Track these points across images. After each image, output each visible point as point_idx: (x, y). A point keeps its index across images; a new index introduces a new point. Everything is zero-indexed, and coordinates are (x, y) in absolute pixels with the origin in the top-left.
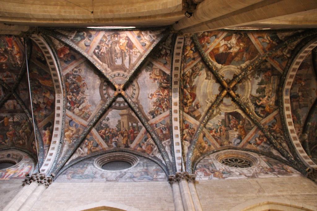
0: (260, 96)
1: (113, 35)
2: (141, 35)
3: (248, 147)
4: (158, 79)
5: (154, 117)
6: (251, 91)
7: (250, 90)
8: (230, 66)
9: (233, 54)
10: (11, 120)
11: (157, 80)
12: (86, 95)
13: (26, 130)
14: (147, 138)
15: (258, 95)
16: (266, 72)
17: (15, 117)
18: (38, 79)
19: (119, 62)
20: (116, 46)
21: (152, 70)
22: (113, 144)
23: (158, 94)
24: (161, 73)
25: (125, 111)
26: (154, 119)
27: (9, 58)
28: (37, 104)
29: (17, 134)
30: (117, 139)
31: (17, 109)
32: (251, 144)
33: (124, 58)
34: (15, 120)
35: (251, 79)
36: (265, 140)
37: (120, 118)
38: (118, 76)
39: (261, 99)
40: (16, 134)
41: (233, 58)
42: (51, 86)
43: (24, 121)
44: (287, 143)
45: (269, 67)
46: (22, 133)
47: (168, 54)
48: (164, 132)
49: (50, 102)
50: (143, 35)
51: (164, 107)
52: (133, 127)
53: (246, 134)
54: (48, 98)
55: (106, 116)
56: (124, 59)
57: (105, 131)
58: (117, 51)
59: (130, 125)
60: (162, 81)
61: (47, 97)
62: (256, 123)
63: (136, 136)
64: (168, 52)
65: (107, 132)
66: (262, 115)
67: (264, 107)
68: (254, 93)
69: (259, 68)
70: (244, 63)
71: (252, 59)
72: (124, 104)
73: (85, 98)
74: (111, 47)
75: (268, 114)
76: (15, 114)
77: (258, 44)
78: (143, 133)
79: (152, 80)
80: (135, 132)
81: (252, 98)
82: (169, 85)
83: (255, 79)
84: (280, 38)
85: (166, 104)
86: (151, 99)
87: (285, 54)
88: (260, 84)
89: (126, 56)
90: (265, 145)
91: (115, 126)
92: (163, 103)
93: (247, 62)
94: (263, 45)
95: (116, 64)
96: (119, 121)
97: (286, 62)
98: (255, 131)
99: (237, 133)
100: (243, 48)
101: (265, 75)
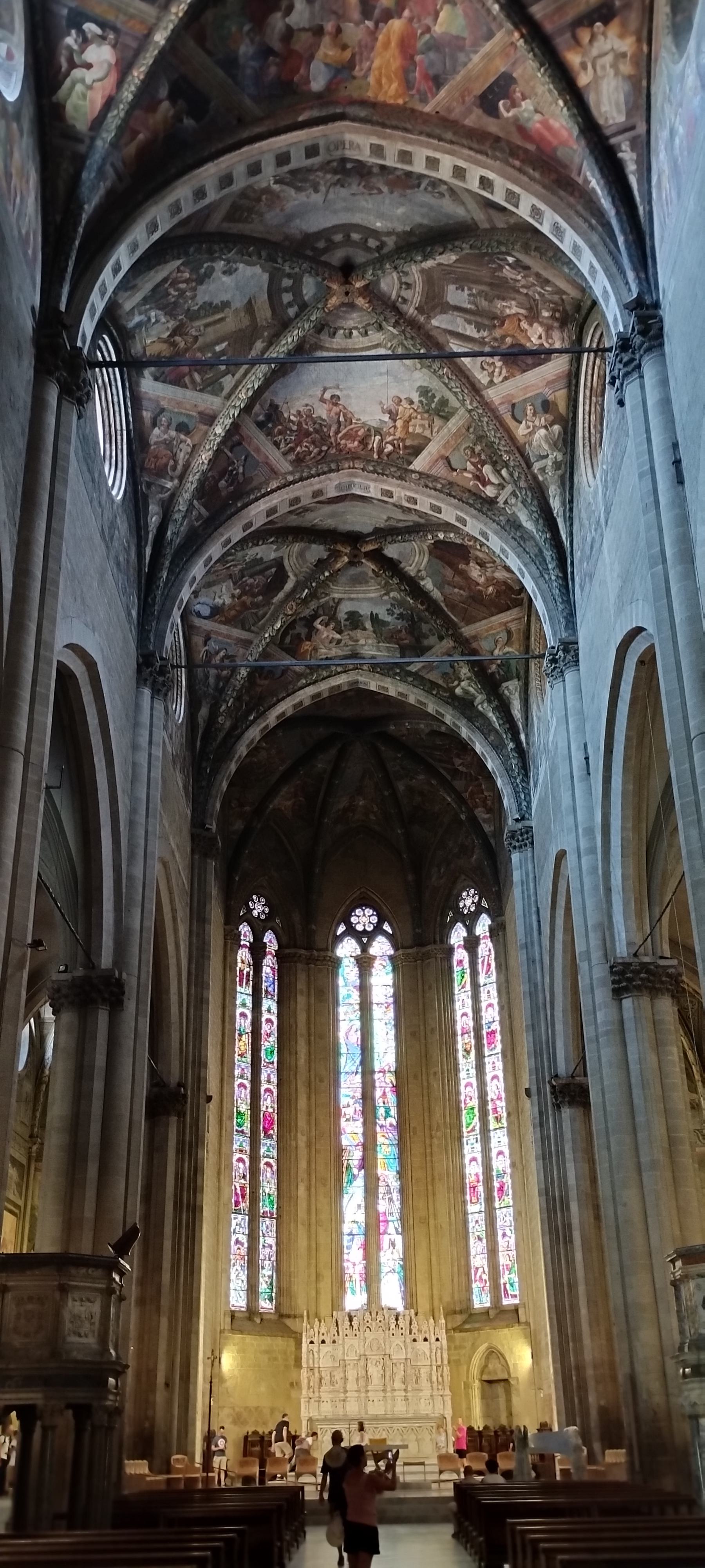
0: (338, 623)
1: (561, 308)
2: (550, 417)
3: (198, 640)
4: (395, 427)
5: (260, 425)
6: (352, 599)
7: (353, 596)
8: (427, 556)
9: (462, 566)
11: (391, 424)
12: (328, 192)
14: (188, 433)
15: (342, 615)
18: (406, 13)
19: (455, 295)
20: (520, 305)
21: (427, 411)
22: (137, 319)
23: (342, 419)
24: (416, 443)
25: (264, 313)
26: (254, 427)
30: (157, 321)
33: (473, 318)
35: (386, 598)
37: (238, 303)
38: (401, 283)
39: (332, 626)
41: (451, 565)
42: (371, 79)
45: (426, 642)
47: (484, 485)
48: (223, 483)
50: (551, 425)
51: (299, 449)
53: (226, 622)
54: (312, 57)
55: (242, 262)
56: (468, 317)
57: (186, 281)
58: (500, 304)
59: (218, 348)
63: (185, 386)
64: (490, 491)
65: (183, 286)
66: (288, 640)
68: (345, 608)
69: (421, 619)
70: (435, 585)
71: (447, 606)
72: (290, 305)
73: (316, 190)
74: (518, 292)
77: (491, 628)
79: (389, 404)
80: (197, 377)
81: (331, 603)
82: (375, 456)
83: (389, 606)
84: (504, 685)
85: (311, 453)
86: (322, 400)
87: (463, 684)
88: (374, 618)
89: (479, 327)
90: (212, 680)
91: (207, 298)
92: (313, 442)
93: (436, 594)
94: (486, 637)
95: (452, 288)
96: (226, 304)
97: (440, 682)
98: (242, 640)
99: (228, 601)
100: (480, 591)
101: (401, 631)
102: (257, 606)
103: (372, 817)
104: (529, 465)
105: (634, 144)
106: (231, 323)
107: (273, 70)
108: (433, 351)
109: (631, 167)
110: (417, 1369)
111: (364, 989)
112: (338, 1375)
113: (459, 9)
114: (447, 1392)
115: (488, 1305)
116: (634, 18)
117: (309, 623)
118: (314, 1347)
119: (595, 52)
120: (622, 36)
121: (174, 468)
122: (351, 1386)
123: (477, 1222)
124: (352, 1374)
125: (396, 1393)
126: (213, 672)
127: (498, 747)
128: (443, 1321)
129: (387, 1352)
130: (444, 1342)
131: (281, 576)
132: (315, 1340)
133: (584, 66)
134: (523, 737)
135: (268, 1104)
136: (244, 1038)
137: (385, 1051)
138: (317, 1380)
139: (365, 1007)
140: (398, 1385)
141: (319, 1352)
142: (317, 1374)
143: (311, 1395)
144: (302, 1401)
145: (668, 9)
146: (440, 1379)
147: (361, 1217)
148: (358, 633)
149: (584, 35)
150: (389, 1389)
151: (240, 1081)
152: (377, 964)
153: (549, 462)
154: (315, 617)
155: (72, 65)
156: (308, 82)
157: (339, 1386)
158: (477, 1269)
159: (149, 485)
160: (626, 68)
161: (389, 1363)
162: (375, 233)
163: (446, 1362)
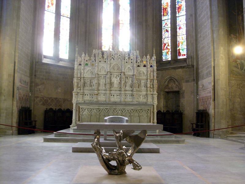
110: (139, 80)
112: (95, 82)
114: (155, 93)
115: (170, 59)
118: (82, 67)
122: (102, 87)
123: (166, 24)
124: (102, 81)
125: (127, 92)
128: (155, 57)
129: (123, 71)
130: (155, 68)
132: (82, 63)
138: (82, 84)
140: (128, 88)
141: (84, 70)
142: (82, 81)
143: (79, 91)
144: (74, 94)
146: (152, 86)
150: (123, 89)
157: (95, 87)
158: (165, 44)
161: (123, 76)
163: (155, 78)
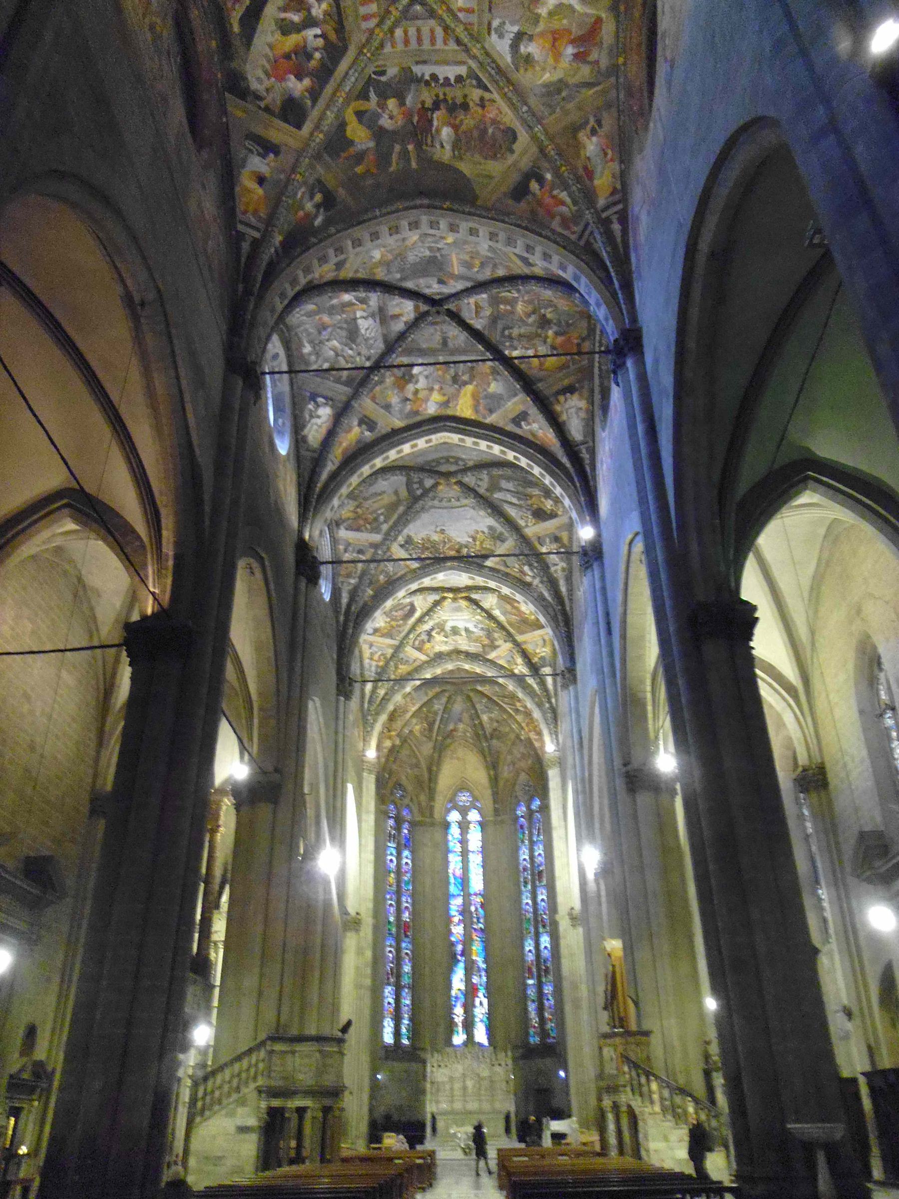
5: (402, 546)
10: (359, 314)
13: (340, 358)
15: (448, 628)
16: (488, 638)
17: (370, 321)
18: (475, 383)
20: (540, 490)
25: (404, 493)
27: (527, 325)
28: (412, 376)
29: (324, 333)
31: (392, 323)
32: (370, 648)
34: (360, 321)
36: (381, 664)
37: (390, 491)
39: (442, 634)
40: (325, 328)
43: (364, 352)
44: (386, 694)
45: (497, 643)
46: (331, 349)
49: (421, 406)
52: (376, 519)
53: (383, 636)
58: (530, 490)
59: (379, 512)
60: (473, 550)
61: (431, 395)
62: (401, 643)
63: (362, 531)
67: (429, 641)
75: (419, 649)
76: (378, 320)
78: (371, 540)
80: (368, 526)
86: (436, 532)
88: (467, 630)
89: (519, 499)
90: (373, 669)
96: (384, 492)
97: (506, 665)
102: (399, 626)
103: (468, 734)
104: (548, 568)
105: (587, 449)
106: (387, 499)
107: (409, 407)
108: (496, 510)
109: (587, 462)
111: (463, 842)
113: (500, 384)
116: (586, 393)
117: (429, 633)
119: (567, 406)
120: (580, 400)
121: (356, 573)
126: (374, 663)
127: (540, 705)
131: (413, 610)
133: (562, 412)
134: (553, 700)
135: (406, 916)
136: (392, 875)
137: (477, 883)
139: (465, 854)
145: (600, 397)
147: (463, 987)
148: (457, 638)
149: (561, 398)
151: (390, 902)
152: (471, 826)
153: (559, 567)
154: (432, 630)
155: (311, 417)
156: (426, 409)
159: (342, 582)
160: (583, 415)
162: (463, 460)
